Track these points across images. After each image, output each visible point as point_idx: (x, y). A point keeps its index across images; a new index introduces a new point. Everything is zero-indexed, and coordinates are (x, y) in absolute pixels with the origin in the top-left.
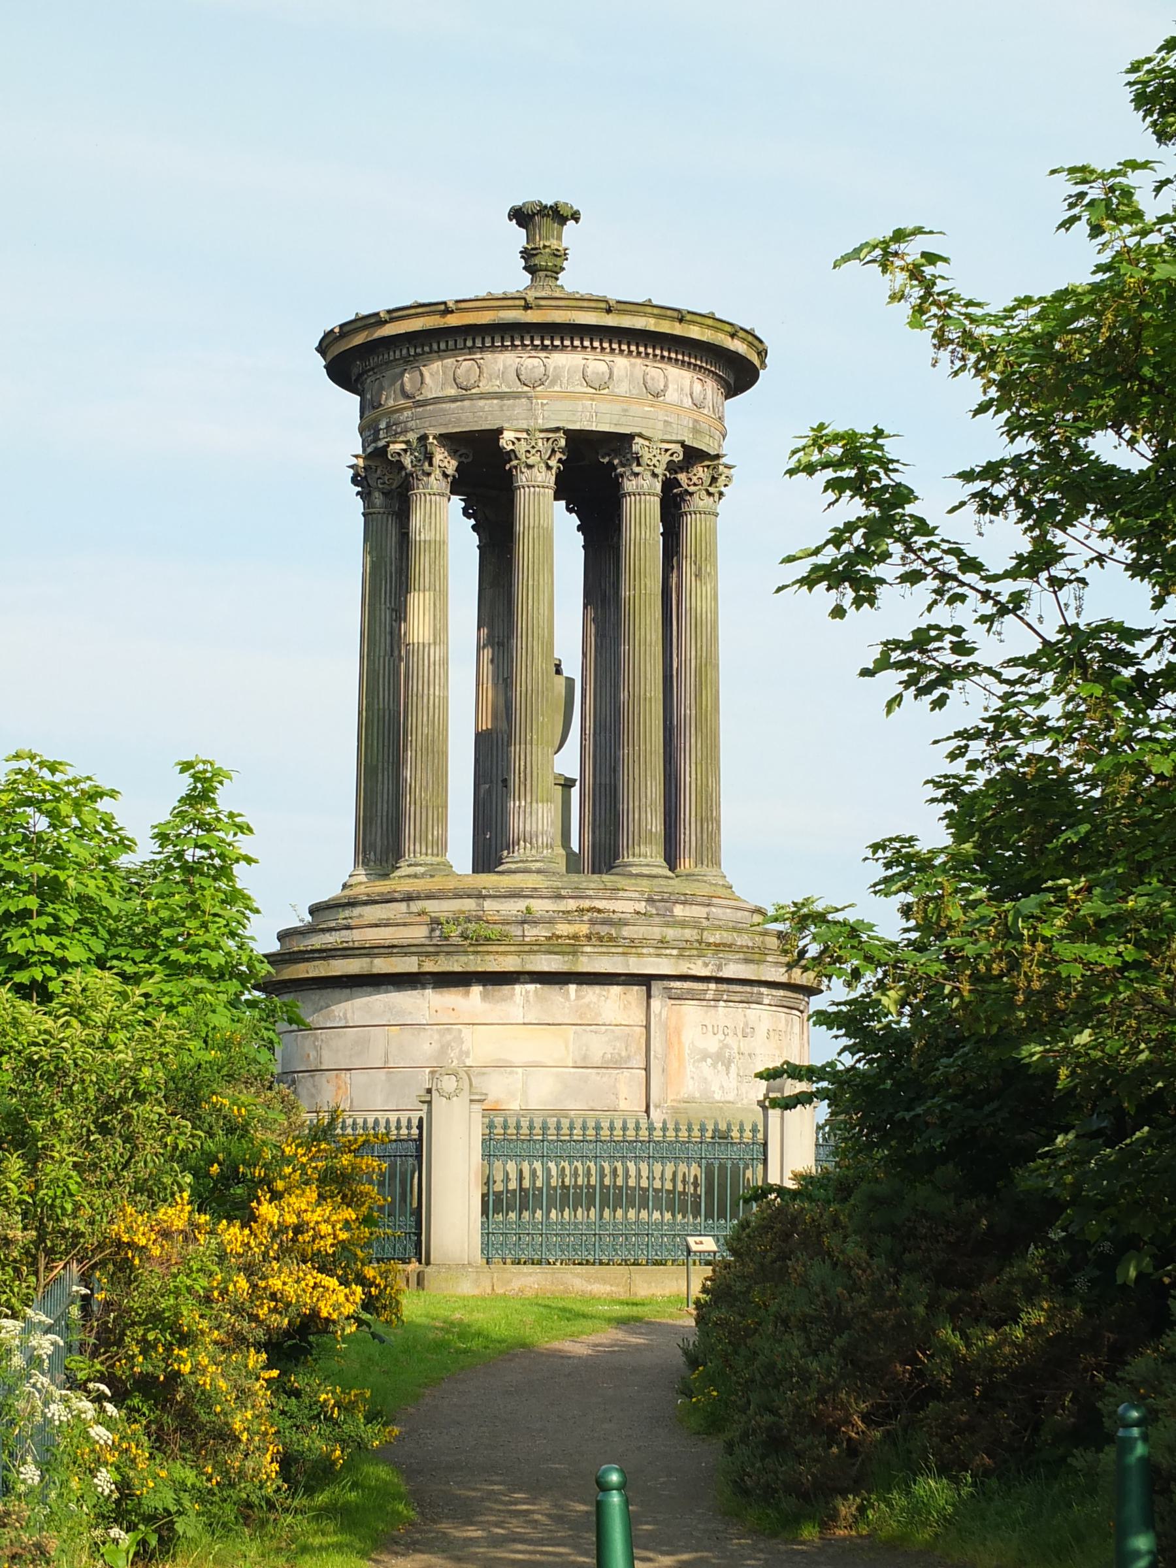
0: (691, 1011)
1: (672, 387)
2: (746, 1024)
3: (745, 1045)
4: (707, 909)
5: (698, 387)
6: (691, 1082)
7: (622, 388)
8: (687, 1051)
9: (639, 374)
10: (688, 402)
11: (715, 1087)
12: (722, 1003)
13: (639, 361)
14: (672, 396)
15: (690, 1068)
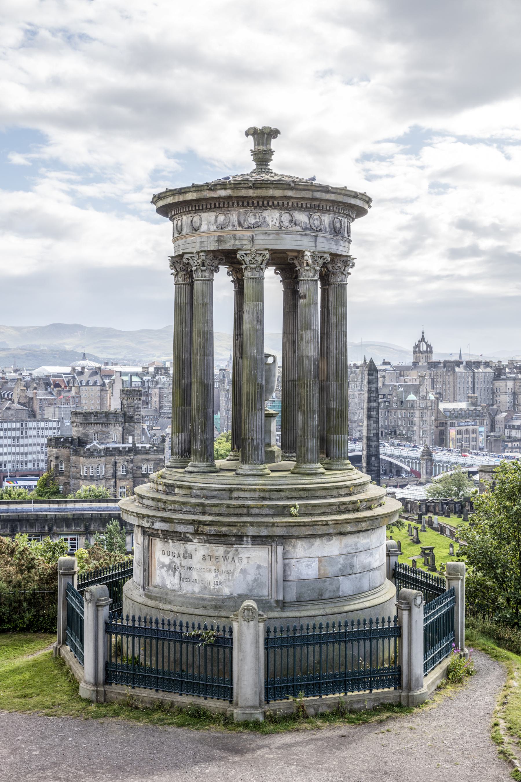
0: (158, 545)
1: (203, 223)
2: (186, 552)
3: (185, 562)
4: (189, 491)
5: (221, 218)
6: (158, 578)
7: (184, 232)
8: (157, 563)
9: (189, 222)
10: (213, 228)
11: (168, 582)
12: (170, 541)
13: (190, 215)
14: (204, 228)
15: (158, 572)
